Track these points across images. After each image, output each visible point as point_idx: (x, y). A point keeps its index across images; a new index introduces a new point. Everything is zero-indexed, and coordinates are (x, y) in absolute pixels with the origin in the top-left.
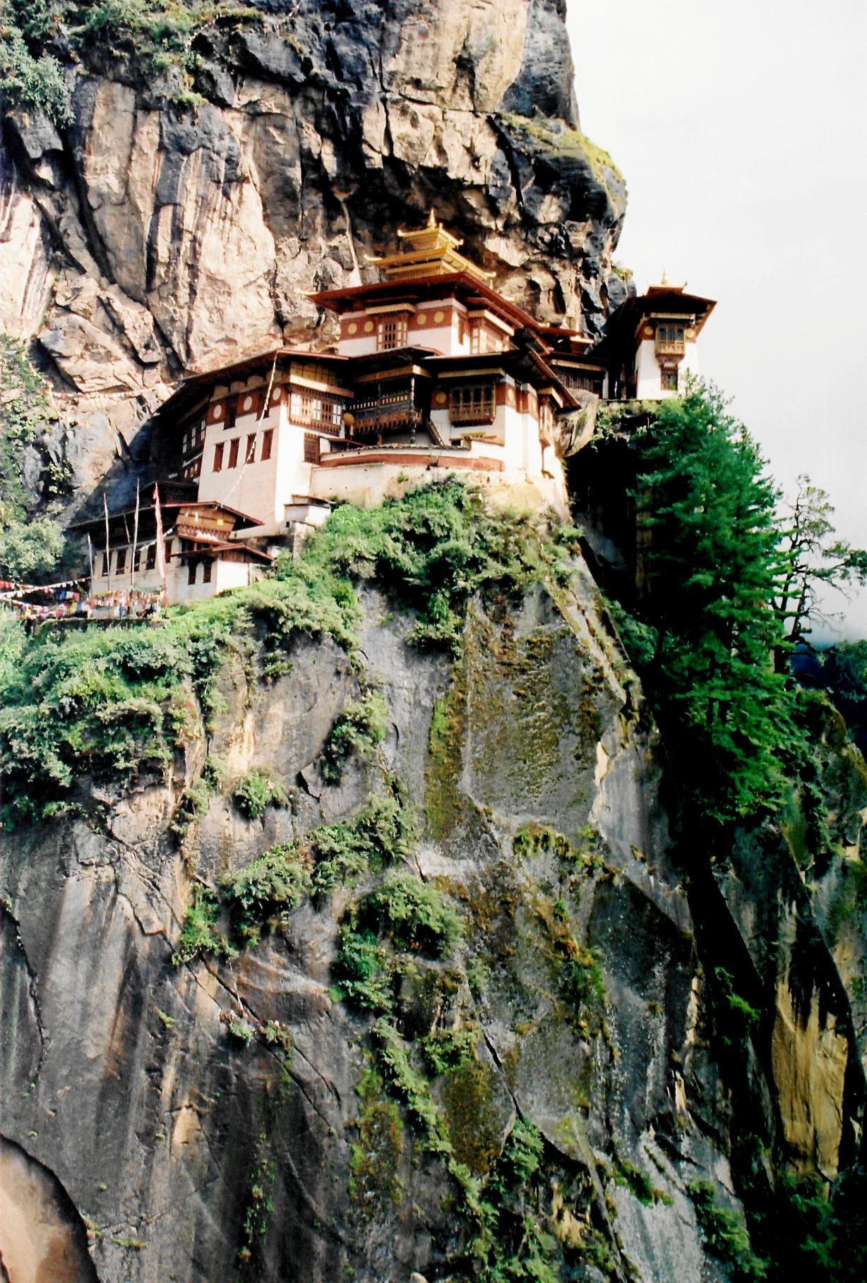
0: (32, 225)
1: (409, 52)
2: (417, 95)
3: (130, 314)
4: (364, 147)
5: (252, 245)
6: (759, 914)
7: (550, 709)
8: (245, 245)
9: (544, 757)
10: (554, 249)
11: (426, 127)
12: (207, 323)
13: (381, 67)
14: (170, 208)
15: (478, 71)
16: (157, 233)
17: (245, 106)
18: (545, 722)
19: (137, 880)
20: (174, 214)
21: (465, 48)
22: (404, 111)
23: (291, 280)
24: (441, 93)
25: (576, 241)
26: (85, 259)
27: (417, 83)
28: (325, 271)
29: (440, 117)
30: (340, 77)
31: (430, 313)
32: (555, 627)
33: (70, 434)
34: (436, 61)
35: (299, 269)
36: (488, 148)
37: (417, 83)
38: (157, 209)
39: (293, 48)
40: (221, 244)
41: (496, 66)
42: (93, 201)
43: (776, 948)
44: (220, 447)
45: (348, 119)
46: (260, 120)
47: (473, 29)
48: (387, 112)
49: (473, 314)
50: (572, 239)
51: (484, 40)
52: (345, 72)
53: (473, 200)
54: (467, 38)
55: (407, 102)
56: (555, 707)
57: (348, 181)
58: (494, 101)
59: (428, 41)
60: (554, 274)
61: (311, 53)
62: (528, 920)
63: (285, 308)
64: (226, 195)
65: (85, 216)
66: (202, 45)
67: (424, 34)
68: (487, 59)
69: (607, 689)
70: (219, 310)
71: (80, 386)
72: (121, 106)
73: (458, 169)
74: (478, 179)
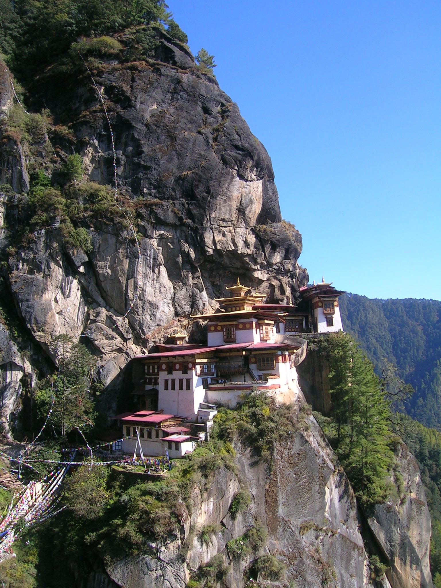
0: (78, 289)
1: (220, 209)
2: (224, 224)
3: (120, 320)
4: (206, 247)
5: (165, 289)
6: (386, 535)
7: (307, 477)
8: (162, 289)
9: (307, 496)
10: (278, 272)
11: (229, 236)
12: (150, 320)
13: (210, 217)
14: (133, 279)
15: (246, 212)
16: (128, 289)
17: (158, 236)
18: (306, 483)
19: (171, 574)
20: (134, 281)
21: (241, 204)
22: (219, 232)
23: (180, 299)
24: (233, 222)
25: (287, 267)
26: (100, 300)
27: (224, 220)
28: (193, 293)
29: (233, 231)
30: (194, 222)
31: (244, 324)
32: (307, 446)
33: (101, 370)
34: (230, 210)
35: (183, 294)
36: (252, 239)
37: (224, 220)
38: (128, 279)
39: (175, 213)
40: (153, 290)
41: (253, 209)
42: (102, 279)
43: (394, 546)
44: (166, 381)
45: (199, 237)
46: (164, 240)
47: (243, 196)
48: (213, 233)
49: (260, 322)
50: (285, 267)
51: (248, 200)
52: (196, 220)
53: (247, 259)
54: (241, 201)
55: (221, 228)
56: (309, 476)
57: (199, 259)
58: (253, 222)
59: (227, 204)
60: (279, 280)
61: (182, 214)
62: (308, 556)
63: (179, 309)
64: (154, 271)
65: (98, 284)
66: (139, 215)
67: (225, 201)
68: (249, 207)
69: (328, 466)
70: (154, 315)
71: (103, 350)
72: (110, 242)
73: (241, 249)
74: (249, 252)
